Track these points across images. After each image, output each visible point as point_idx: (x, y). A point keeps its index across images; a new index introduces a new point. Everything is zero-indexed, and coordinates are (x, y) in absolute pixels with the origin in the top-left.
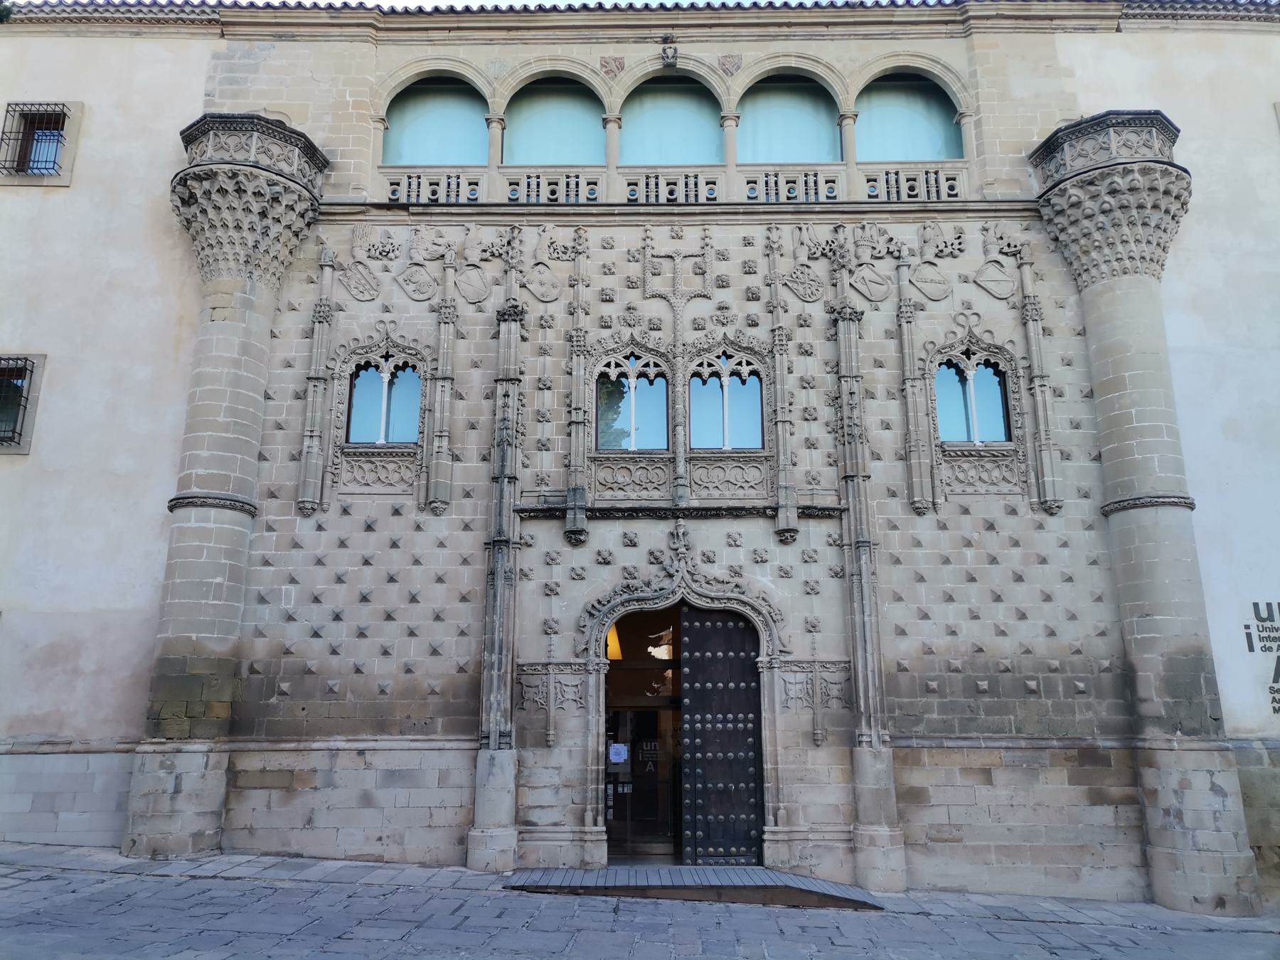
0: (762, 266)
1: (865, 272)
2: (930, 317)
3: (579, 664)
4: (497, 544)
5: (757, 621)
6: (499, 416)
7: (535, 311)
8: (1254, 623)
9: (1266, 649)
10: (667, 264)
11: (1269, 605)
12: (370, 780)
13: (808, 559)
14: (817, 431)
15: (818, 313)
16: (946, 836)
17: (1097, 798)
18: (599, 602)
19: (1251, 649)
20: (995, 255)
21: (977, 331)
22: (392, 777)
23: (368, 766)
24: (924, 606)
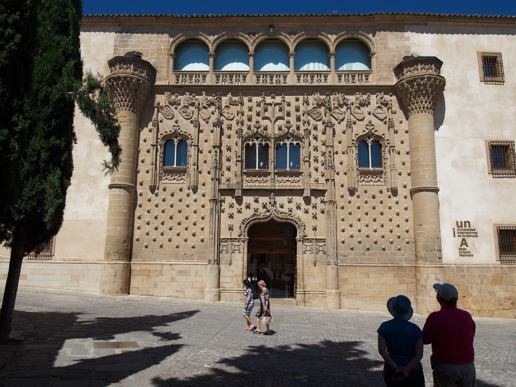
0: (302, 108)
1: (337, 111)
2: (358, 125)
3: (240, 239)
4: (214, 201)
6: (214, 158)
7: (226, 123)
8: (456, 228)
9: (458, 236)
10: (269, 107)
11: (461, 222)
12: (174, 273)
13: (315, 207)
14: (319, 165)
15: (320, 124)
16: (353, 293)
17: (402, 282)
18: (246, 219)
19: (454, 236)
20: (379, 105)
21: (373, 131)
22: (181, 273)
23: (173, 269)
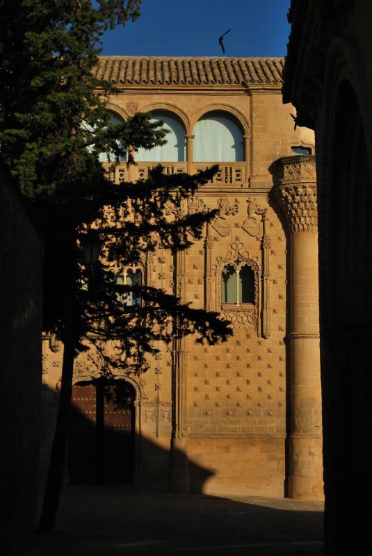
2: (221, 245)
5: (134, 384)
17: (271, 458)
21: (241, 252)
24: (207, 378)
